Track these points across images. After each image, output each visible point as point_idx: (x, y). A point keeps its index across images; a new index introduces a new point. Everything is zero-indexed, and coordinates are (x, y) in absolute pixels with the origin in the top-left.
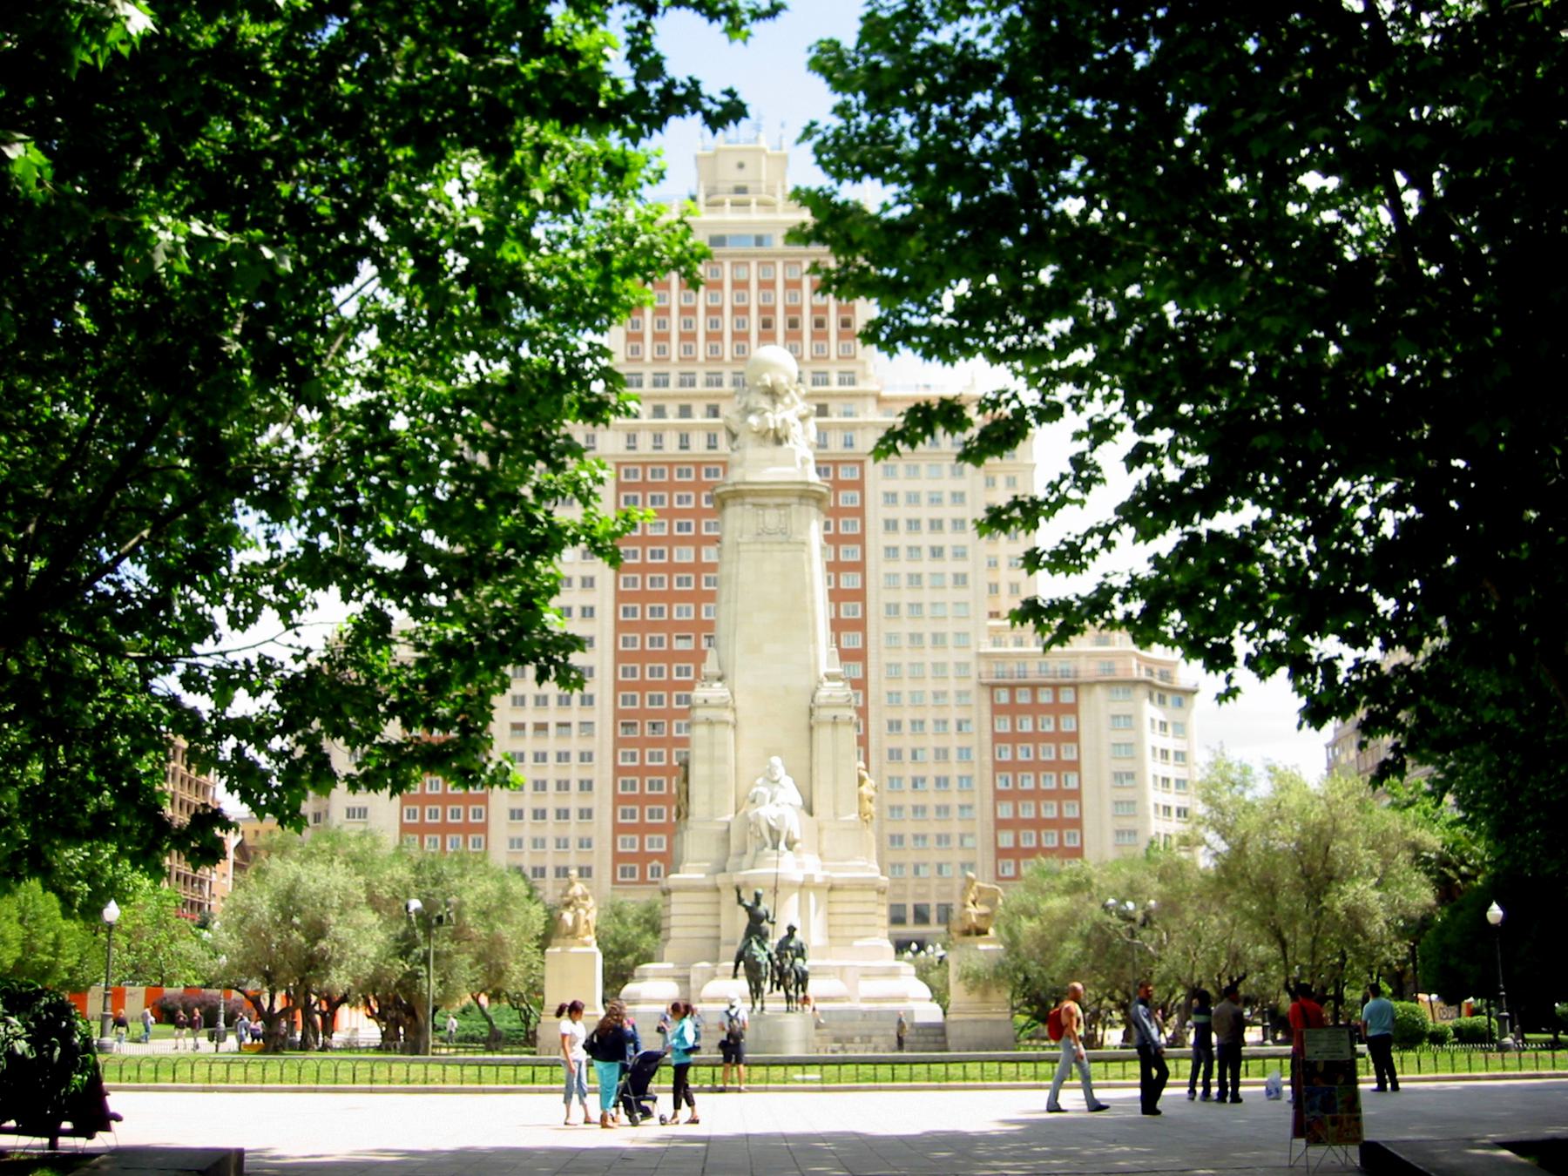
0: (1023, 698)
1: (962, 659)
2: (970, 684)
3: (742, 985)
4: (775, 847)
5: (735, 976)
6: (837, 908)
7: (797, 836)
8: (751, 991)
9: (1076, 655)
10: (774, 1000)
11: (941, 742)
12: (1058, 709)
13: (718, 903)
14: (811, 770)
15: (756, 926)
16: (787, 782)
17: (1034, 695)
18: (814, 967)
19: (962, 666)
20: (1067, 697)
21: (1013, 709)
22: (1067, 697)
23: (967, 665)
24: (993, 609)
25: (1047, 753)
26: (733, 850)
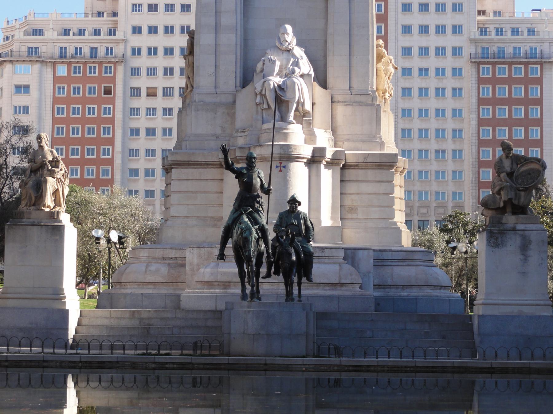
0: (503, 72)
1: (457, 44)
2: (463, 62)
3: (230, 268)
4: (284, 119)
5: (222, 256)
6: (352, 188)
7: (308, 107)
8: (241, 274)
9: (542, 41)
10: (272, 286)
11: (440, 104)
12: (527, 81)
13: (223, 180)
14: (326, 42)
15: (247, 200)
16: (299, 52)
17: (510, 70)
18: (323, 249)
19: (457, 51)
20: (535, 71)
21: (494, 81)
22: (535, 71)
23: (460, 49)
24: (480, 9)
25: (519, 112)
26: (239, 124)
